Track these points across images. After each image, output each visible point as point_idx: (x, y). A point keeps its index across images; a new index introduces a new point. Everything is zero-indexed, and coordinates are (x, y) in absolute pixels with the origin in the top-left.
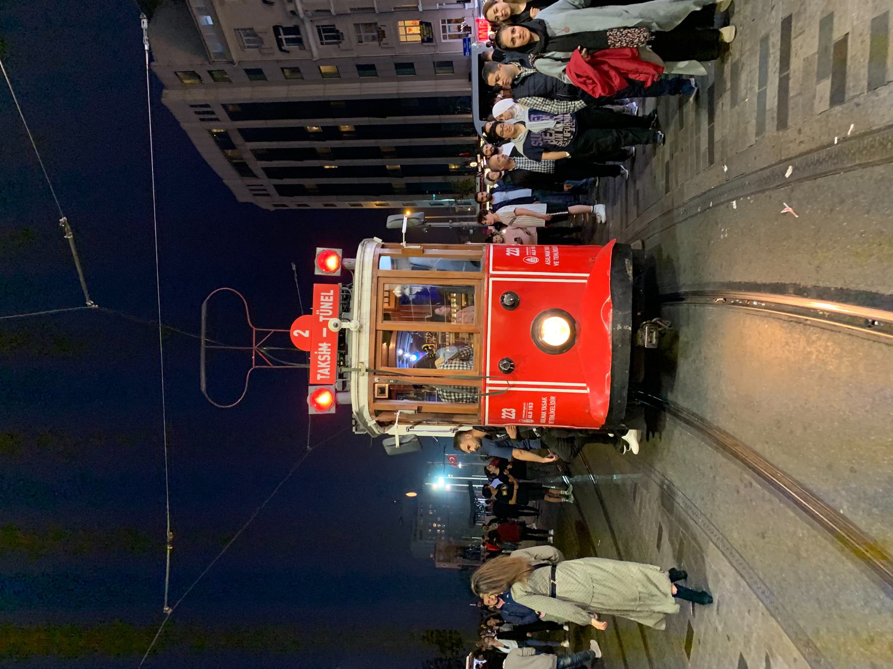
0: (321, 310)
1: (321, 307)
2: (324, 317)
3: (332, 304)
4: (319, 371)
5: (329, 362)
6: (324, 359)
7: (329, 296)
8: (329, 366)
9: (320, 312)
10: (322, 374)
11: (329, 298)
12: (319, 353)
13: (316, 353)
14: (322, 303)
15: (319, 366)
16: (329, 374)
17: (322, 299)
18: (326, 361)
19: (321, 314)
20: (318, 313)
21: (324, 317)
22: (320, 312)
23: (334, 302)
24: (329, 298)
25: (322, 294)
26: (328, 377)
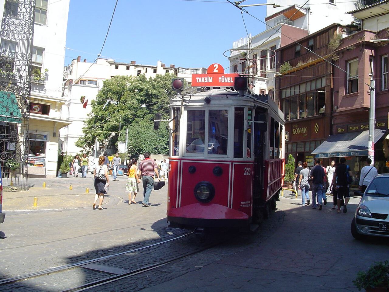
0: (224, 78)
1: (225, 78)
2: (221, 79)
3: (227, 82)
4: (200, 78)
5: (204, 82)
6: (205, 79)
7: (230, 81)
8: (202, 82)
9: (223, 78)
10: (199, 79)
11: (229, 81)
12: (208, 78)
13: (208, 77)
14: (227, 78)
15: (202, 78)
16: (199, 82)
17: (229, 78)
18: (204, 80)
19: (222, 78)
20: (222, 77)
21: (221, 79)
22: (223, 78)
23: (228, 83)
24: (229, 81)
25: (231, 78)
26: (197, 82)
